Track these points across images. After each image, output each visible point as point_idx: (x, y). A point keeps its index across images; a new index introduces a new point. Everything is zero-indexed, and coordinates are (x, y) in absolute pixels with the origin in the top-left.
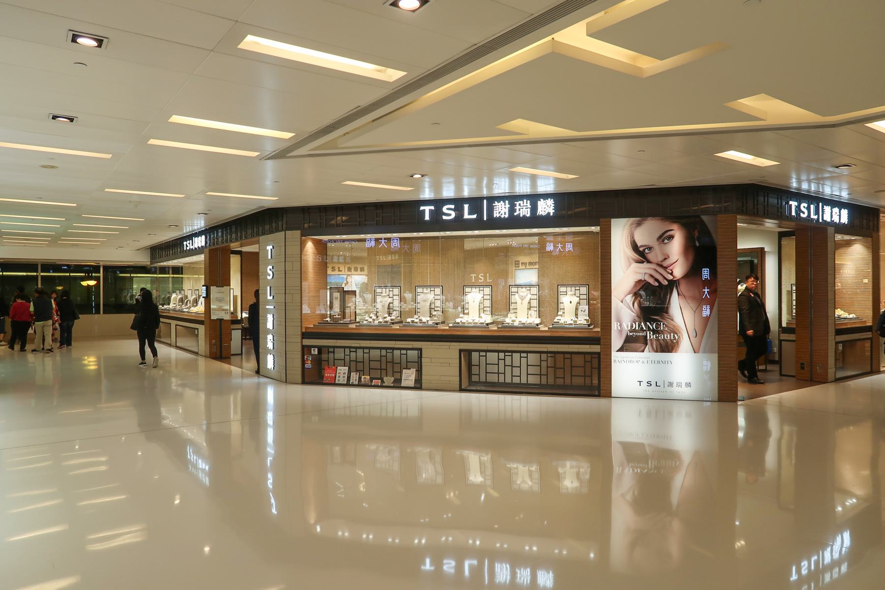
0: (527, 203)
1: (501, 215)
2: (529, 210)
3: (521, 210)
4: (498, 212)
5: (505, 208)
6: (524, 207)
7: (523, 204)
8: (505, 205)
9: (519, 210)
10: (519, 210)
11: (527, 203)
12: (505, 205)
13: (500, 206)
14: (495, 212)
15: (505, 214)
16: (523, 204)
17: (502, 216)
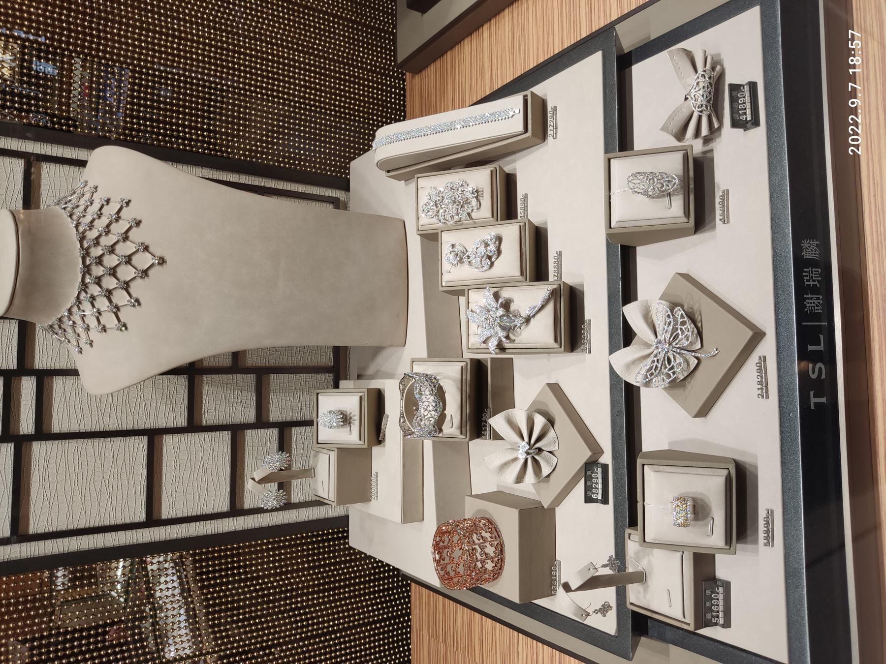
0: (806, 272)
1: (819, 303)
2: (813, 269)
3: (814, 279)
4: (816, 308)
5: (812, 298)
6: (811, 274)
7: (807, 276)
8: (808, 298)
9: (814, 281)
10: (814, 281)
11: (806, 272)
12: (808, 298)
13: (810, 305)
14: (816, 311)
15: (818, 299)
16: (807, 276)
17: (821, 302)
